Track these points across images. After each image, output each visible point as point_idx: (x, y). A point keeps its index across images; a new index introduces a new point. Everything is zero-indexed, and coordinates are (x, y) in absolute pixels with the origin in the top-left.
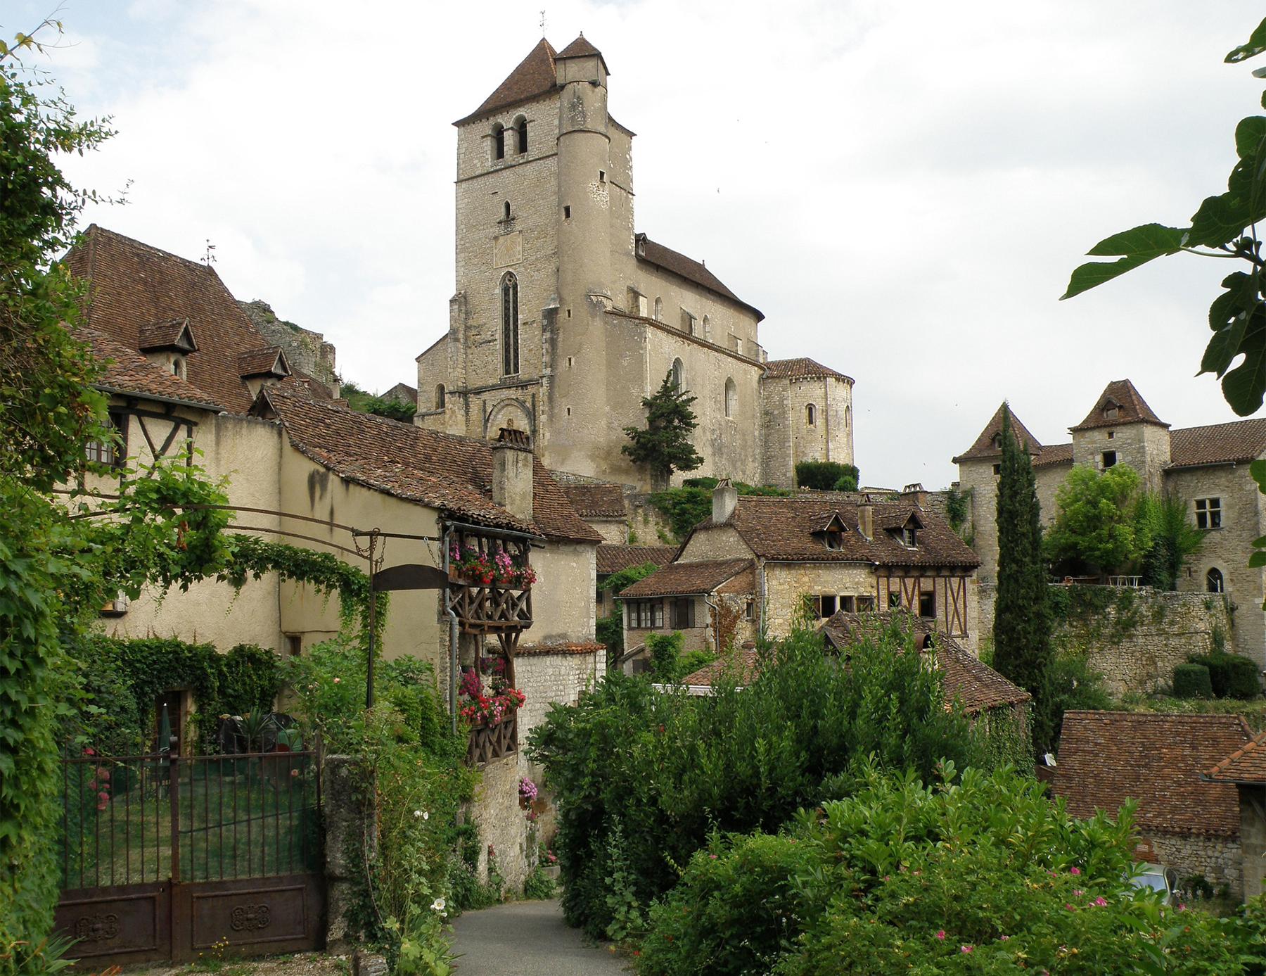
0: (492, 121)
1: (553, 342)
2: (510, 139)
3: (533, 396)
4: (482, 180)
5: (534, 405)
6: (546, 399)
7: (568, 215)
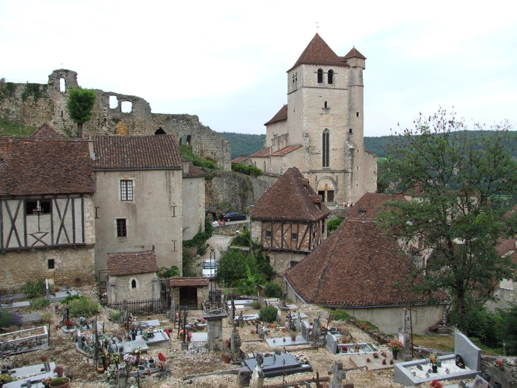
0: (319, 67)
1: (352, 160)
2: (326, 76)
3: (337, 176)
4: (315, 90)
5: (337, 180)
6: (350, 180)
7: (357, 115)
